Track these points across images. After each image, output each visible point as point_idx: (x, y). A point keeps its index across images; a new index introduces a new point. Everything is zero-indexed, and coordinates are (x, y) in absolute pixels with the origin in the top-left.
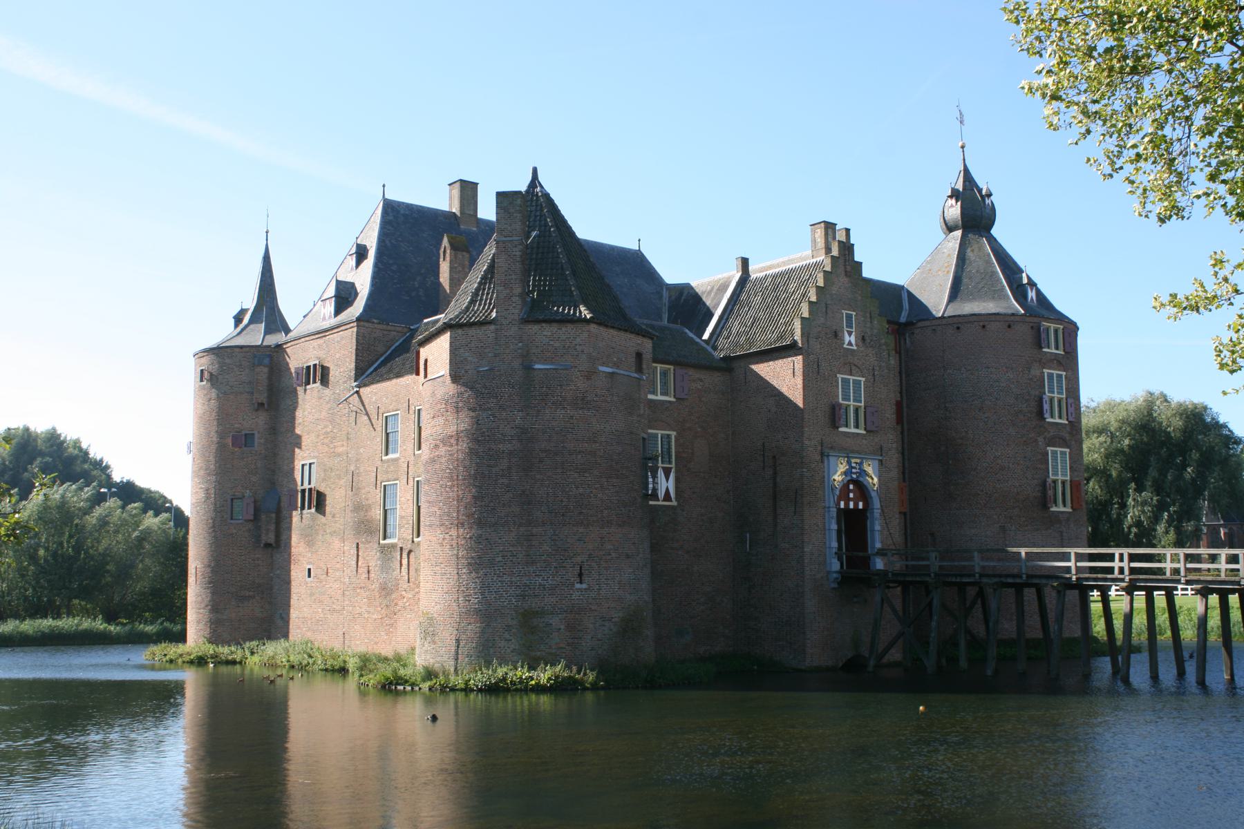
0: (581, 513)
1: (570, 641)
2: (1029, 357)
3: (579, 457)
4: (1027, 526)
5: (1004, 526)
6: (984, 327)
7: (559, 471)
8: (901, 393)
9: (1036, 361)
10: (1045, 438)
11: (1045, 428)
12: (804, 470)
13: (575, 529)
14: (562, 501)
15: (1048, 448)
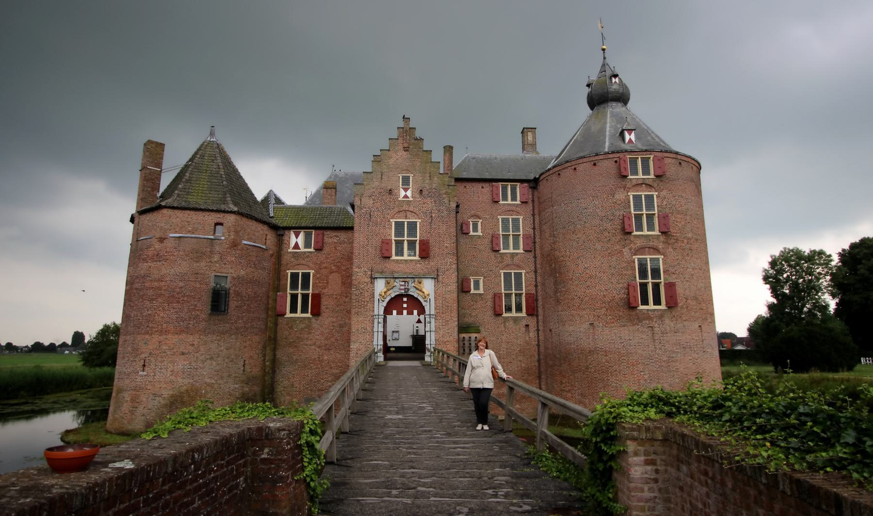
0: (148, 326)
1: (131, 409)
2: (613, 185)
3: (151, 291)
4: (613, 323)
5: (593, 324)
6: (575, 169)
7: (141, 300)
8: (534, 229)
9: (621, 188)
10: (630, 249)
11: (630, 240)
12: (353, 289)
13: (144, 336)
14: (139, 319)
15: (634, 257)
